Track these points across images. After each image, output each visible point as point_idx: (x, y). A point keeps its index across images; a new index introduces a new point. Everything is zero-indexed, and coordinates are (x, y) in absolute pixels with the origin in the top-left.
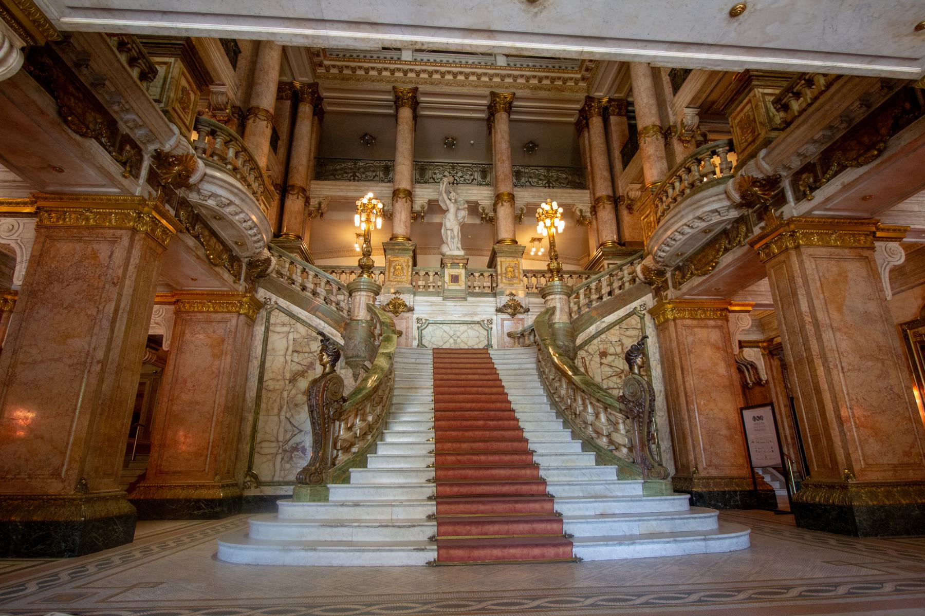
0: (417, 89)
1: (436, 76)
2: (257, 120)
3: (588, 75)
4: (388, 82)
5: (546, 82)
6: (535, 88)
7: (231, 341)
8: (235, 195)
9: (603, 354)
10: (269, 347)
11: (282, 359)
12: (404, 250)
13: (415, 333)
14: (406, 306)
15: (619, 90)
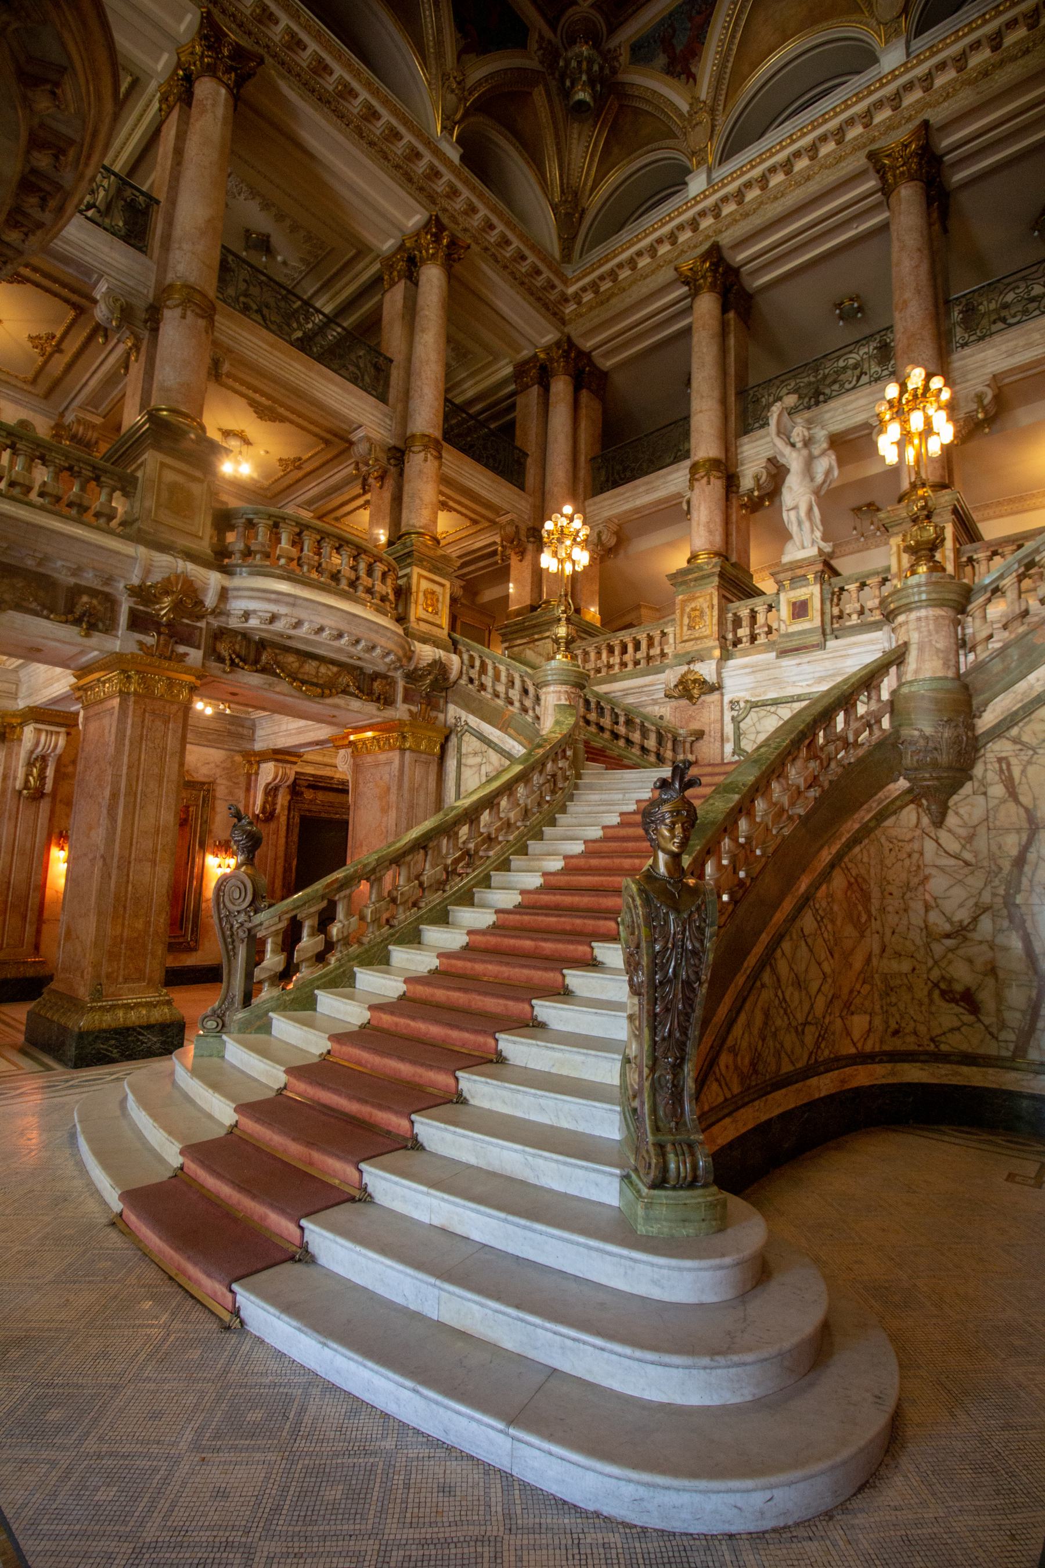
8: (276, 602)
12: (703, 577)
13: (729, 729)
14: (705, 682)
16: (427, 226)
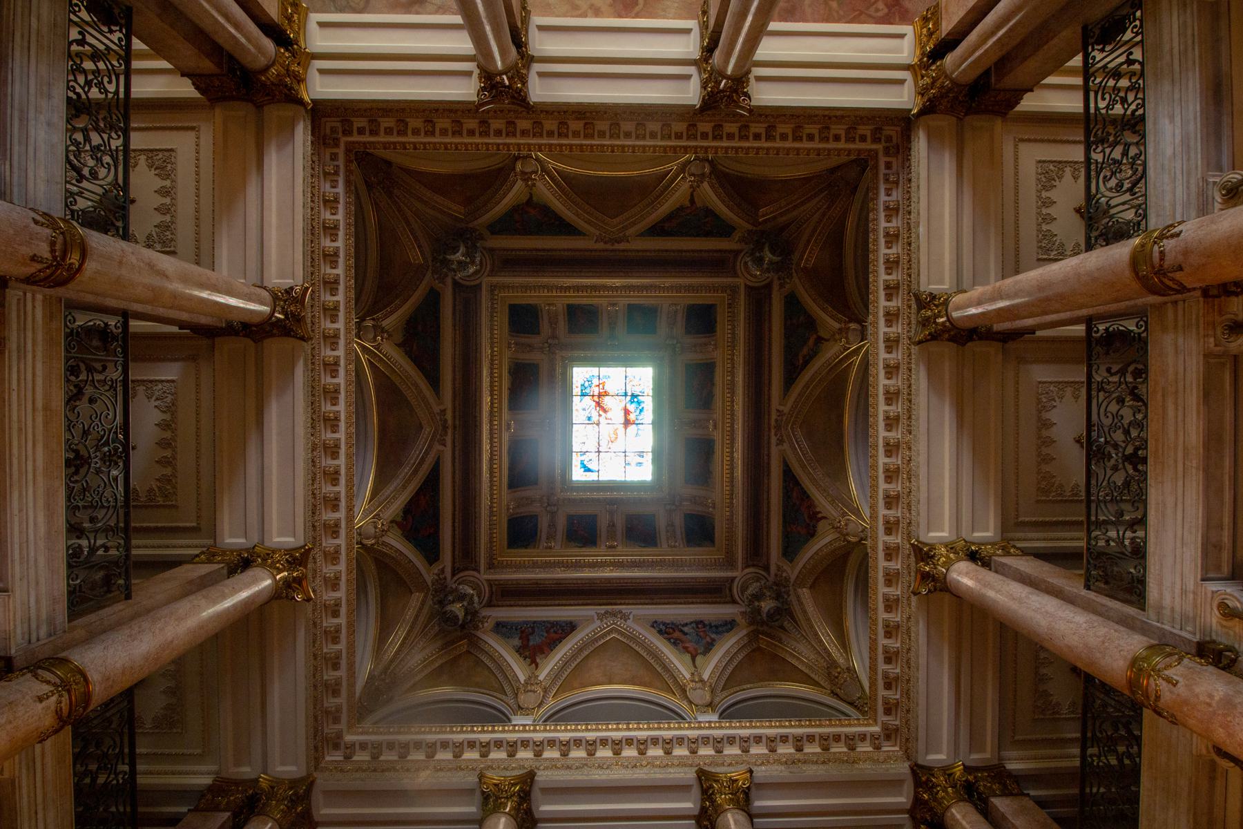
0: (530, 776)
3: (894, 721)
5: (812, 749)
6: (790, 762)
15: (975, 742)
16: (290, 551)
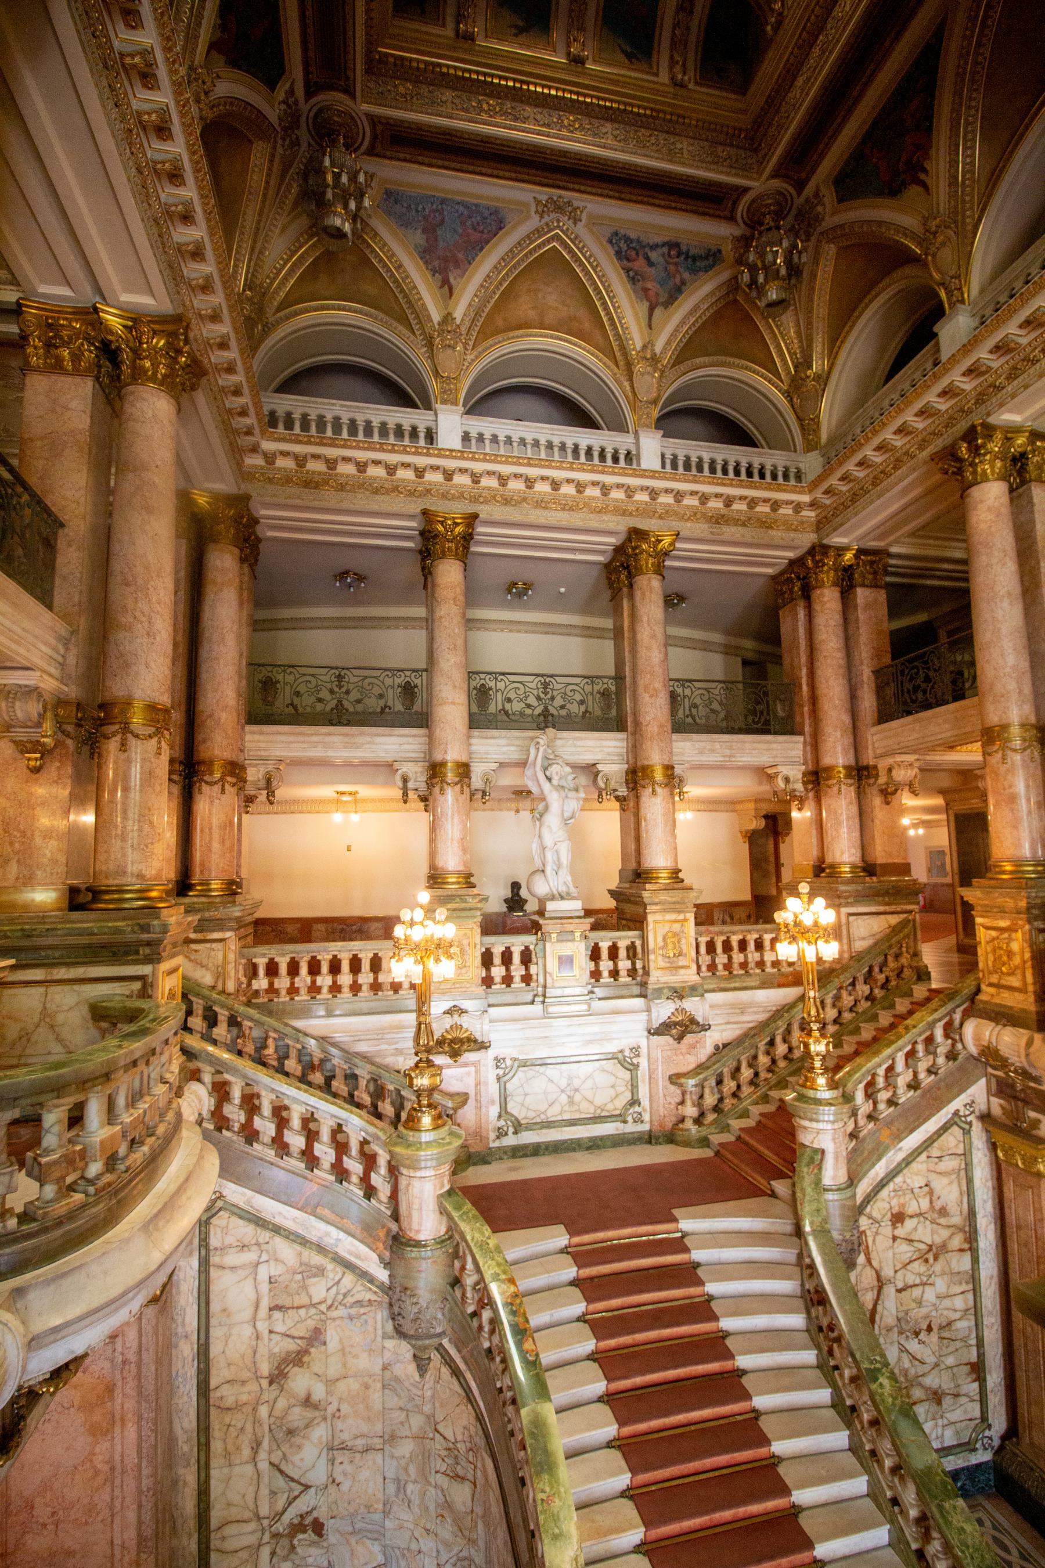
0: (476, 516)
1: (516, 486)
2: (132, 741)
4: (411, 493)
6: (718, 520)
7: (130, 1388)
9: (898, 1218)
10: (215, 1307)
11: (248, 1331)
13: (492, 1089)
15: (881, 537)
